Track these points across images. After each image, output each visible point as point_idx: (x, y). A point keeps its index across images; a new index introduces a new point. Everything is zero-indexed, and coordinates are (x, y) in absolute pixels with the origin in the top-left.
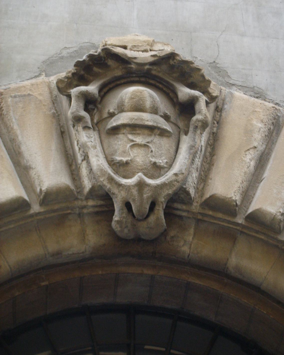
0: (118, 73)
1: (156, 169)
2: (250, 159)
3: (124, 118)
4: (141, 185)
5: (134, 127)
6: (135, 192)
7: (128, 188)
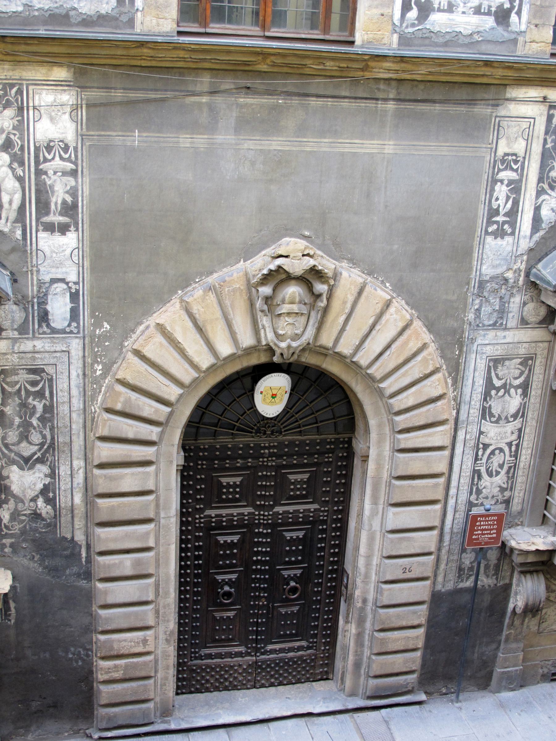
0: (284, 276)
1: (296, 337)
2: (342, 319)
3: (285, 308)
4: (289, 347)
5: (289, 314)
6: (286, 351)
7: (283, 349)
